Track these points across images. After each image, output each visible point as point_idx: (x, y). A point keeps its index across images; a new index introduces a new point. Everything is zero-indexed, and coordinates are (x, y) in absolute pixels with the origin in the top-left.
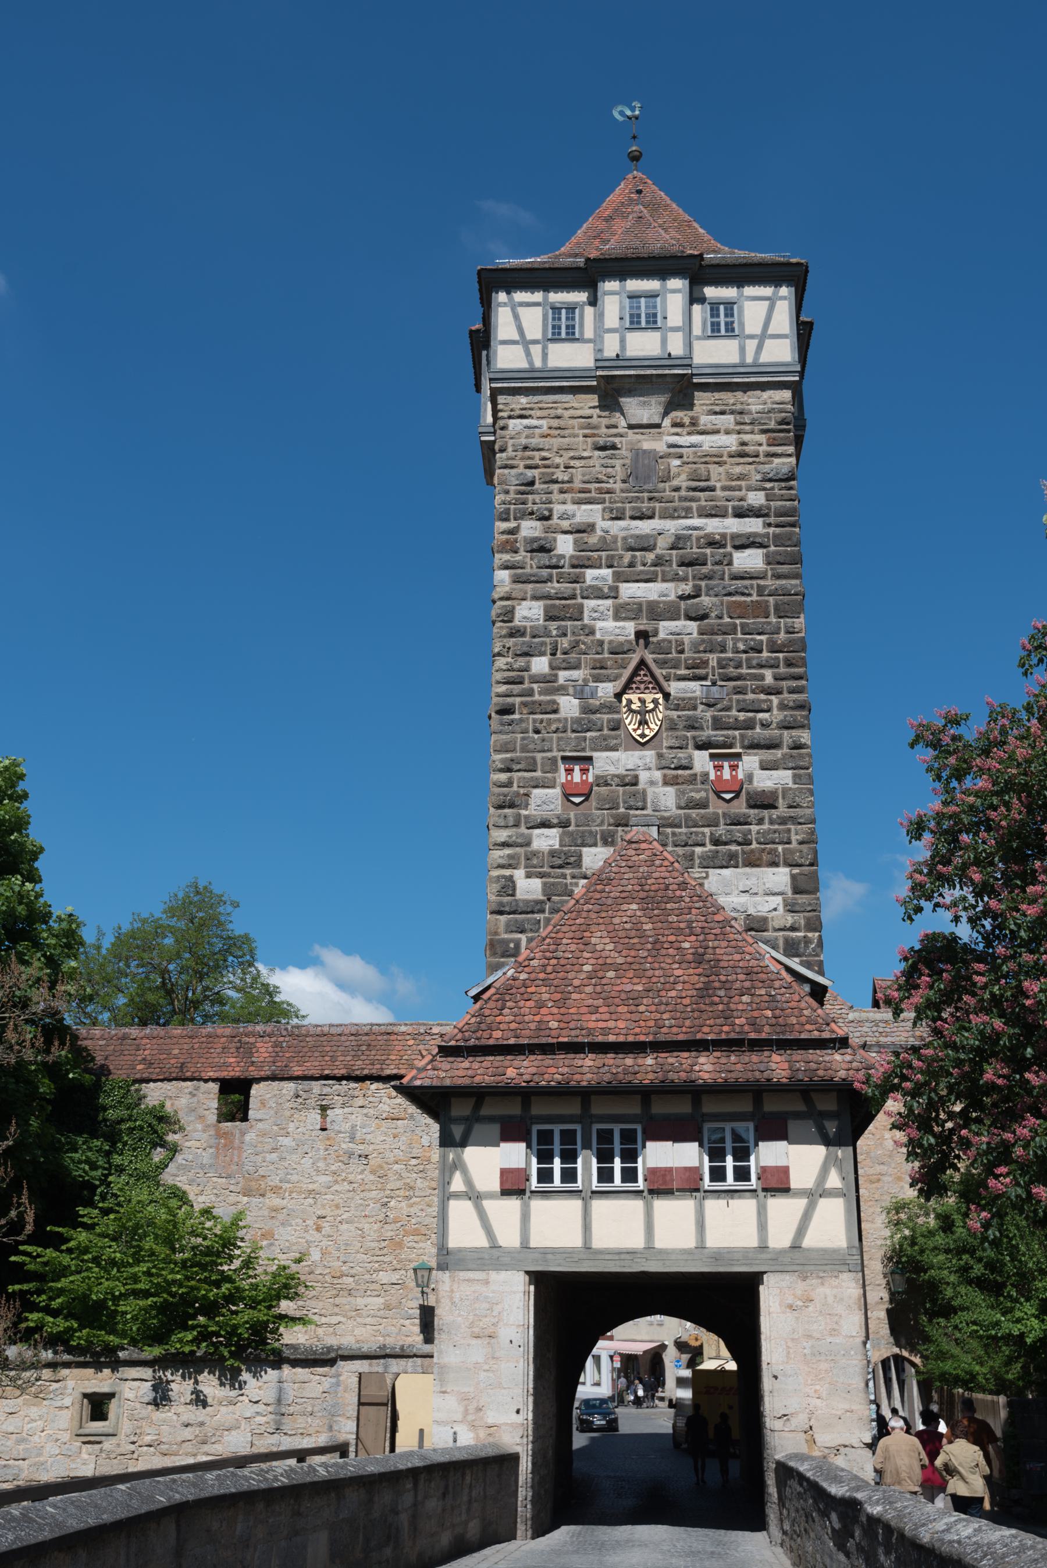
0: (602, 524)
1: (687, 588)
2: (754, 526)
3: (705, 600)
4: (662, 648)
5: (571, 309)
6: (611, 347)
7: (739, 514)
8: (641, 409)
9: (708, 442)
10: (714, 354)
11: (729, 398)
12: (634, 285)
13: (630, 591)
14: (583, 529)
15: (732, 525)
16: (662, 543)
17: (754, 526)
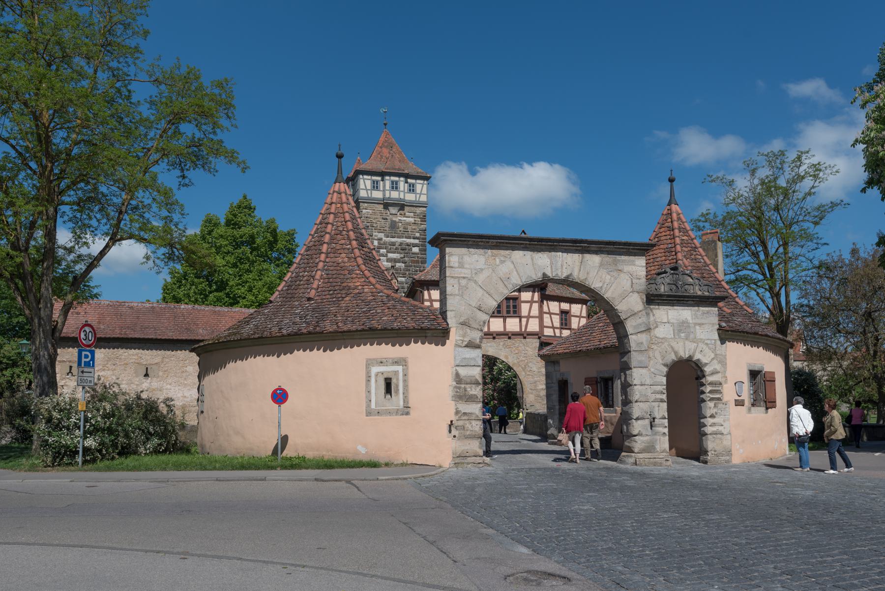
0: (384, 239)
1: (402, 256)
2: (417, 241)
3: (406, 259)
4: (397, 269)
5: (377, 182)
6: (387, 195)
7: (414, 238)
8: (393, 210)
9: (408, 220)
10: (410, 197)
11: (413, 209)
12: (393, 178)
13: (390, 255)
14: (380, 239)
15: (412, 241)
16: (397, 244)
17: (417, 241)
